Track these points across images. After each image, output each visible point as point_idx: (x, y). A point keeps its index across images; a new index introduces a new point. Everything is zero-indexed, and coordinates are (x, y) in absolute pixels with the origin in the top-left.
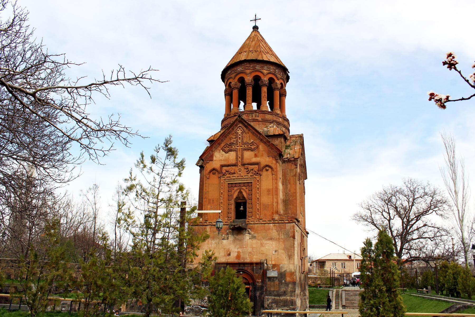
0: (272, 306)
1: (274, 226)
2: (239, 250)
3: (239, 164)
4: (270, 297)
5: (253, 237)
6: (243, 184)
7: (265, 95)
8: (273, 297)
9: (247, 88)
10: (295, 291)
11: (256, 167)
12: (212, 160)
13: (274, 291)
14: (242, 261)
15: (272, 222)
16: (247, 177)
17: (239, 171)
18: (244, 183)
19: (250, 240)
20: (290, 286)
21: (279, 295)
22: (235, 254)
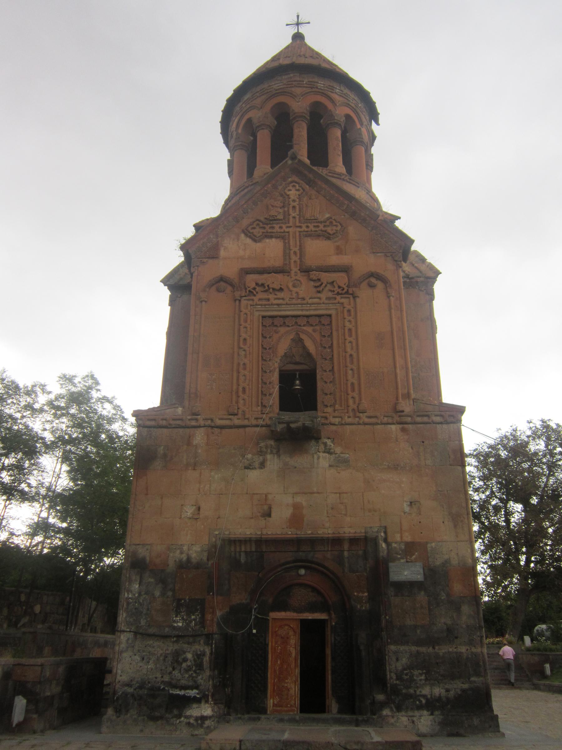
1: (403, 430)
2: (298, 499)
3: (294, 269)
4: (402, 648)
5: (341, 463)
8: (414, 649)
9: (295, 126)
11: (341, 279)
14: (306, 532)
15: (396, 419)
17: (294, 286)
18: (308, 316)
20: (466, 609)
21: (433, 641)
22: (287, 513)
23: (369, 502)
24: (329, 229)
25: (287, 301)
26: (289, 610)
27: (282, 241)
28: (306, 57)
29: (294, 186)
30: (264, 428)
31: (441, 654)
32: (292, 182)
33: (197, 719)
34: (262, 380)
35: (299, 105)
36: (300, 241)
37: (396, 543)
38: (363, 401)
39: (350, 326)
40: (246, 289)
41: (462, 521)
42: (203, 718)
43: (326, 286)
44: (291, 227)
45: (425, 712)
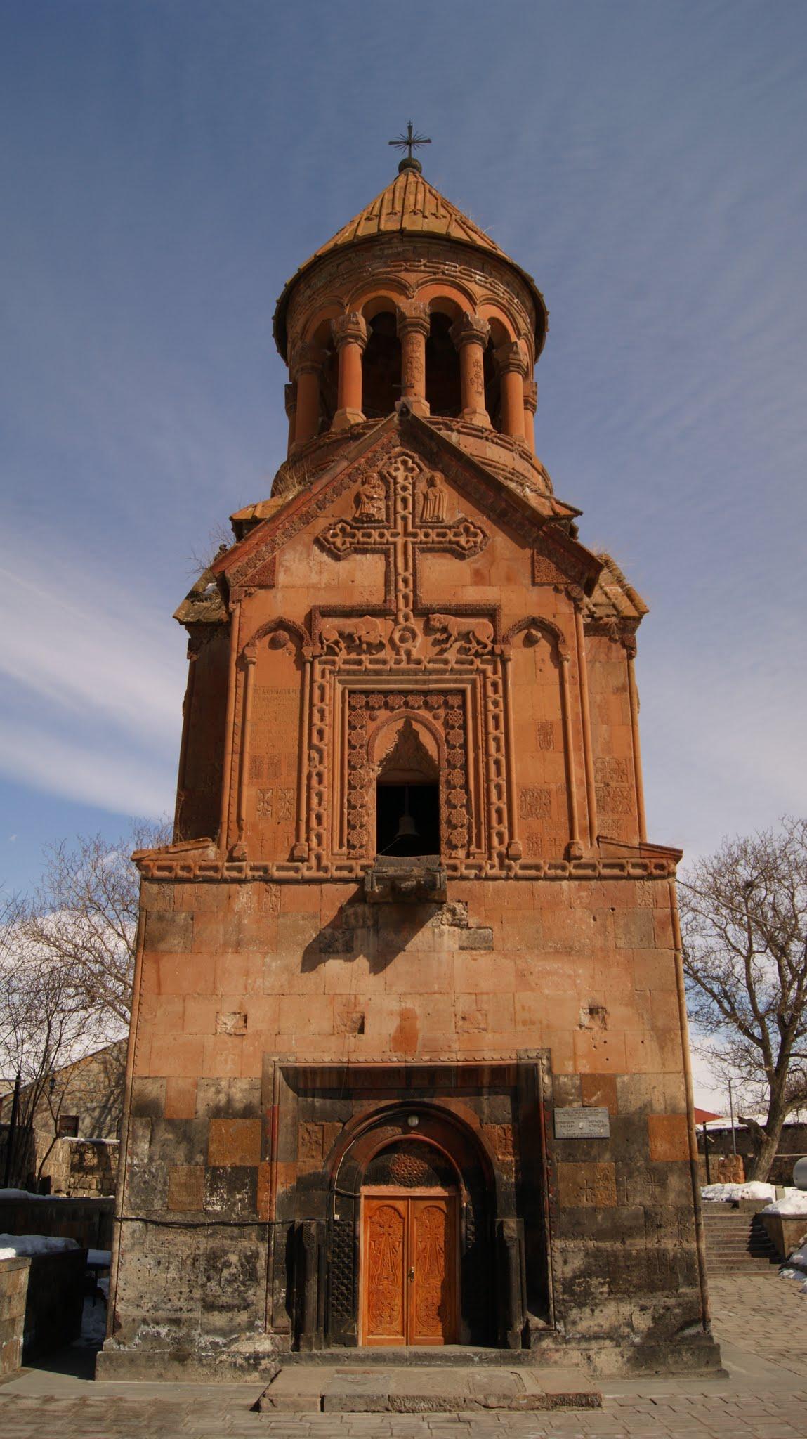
0: (587, 1293)
2: (409, 1004)
4: (571, 1244)
5: (478, 944)
6: (420, 700)
7: (477, 375)
8: (591, 1244)
10: (697, 1211)
11: (482, 628)
12: (268, 585)
13: (594, 1209)
14: (422, 1058)
19: (465, 955)
21: (621, 1232)
22: (392, 1026)
23: (523, 1008)
24: (463, 540)
26: (393, 1183)
27: (383, 557)
28: (425, 217)
29: (404, 463)
30: (352, 885)
31: (634, 1252)
32: (400, 455)
33: (247, 1359)
34: (349, 801)
35: (415, 304)
36: (414, 560)
37: (566, 1076)
38: (516, 839)
39: (497, 711)
40: (322, 643)
41: (672, 1040)
42: (257, 1358)
43: (456, 640)
44: (398, 534)
45: (607, 1343)
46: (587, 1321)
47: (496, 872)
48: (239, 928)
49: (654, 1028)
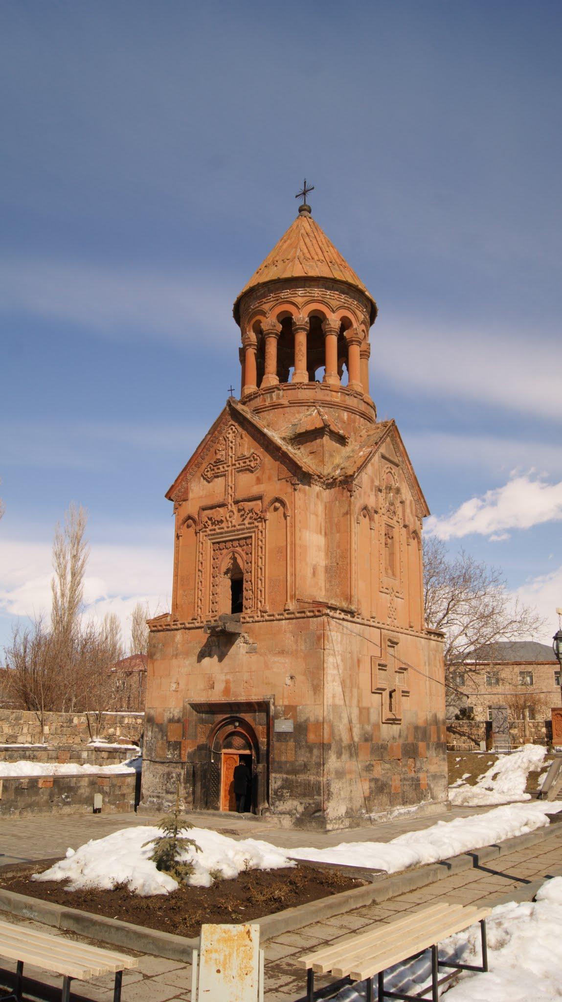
0: (282, 796)
2: (228, 677)
4: (278, 776)
5: (252, 651)
8: (285, 776)
11: (257, 505)
13: (286, 762)
14: (232, 699)
16: (242, 527)
20: (315, 752)
21: (295, 772)
25: (226, 529)
46: (282, 806)
47: (260, 619)
48: (177, 649)
49: (313, 685)
